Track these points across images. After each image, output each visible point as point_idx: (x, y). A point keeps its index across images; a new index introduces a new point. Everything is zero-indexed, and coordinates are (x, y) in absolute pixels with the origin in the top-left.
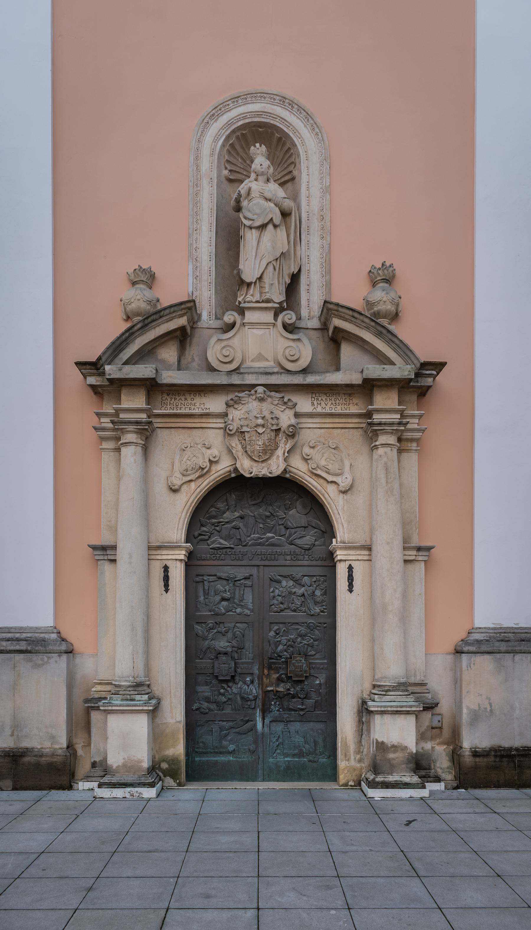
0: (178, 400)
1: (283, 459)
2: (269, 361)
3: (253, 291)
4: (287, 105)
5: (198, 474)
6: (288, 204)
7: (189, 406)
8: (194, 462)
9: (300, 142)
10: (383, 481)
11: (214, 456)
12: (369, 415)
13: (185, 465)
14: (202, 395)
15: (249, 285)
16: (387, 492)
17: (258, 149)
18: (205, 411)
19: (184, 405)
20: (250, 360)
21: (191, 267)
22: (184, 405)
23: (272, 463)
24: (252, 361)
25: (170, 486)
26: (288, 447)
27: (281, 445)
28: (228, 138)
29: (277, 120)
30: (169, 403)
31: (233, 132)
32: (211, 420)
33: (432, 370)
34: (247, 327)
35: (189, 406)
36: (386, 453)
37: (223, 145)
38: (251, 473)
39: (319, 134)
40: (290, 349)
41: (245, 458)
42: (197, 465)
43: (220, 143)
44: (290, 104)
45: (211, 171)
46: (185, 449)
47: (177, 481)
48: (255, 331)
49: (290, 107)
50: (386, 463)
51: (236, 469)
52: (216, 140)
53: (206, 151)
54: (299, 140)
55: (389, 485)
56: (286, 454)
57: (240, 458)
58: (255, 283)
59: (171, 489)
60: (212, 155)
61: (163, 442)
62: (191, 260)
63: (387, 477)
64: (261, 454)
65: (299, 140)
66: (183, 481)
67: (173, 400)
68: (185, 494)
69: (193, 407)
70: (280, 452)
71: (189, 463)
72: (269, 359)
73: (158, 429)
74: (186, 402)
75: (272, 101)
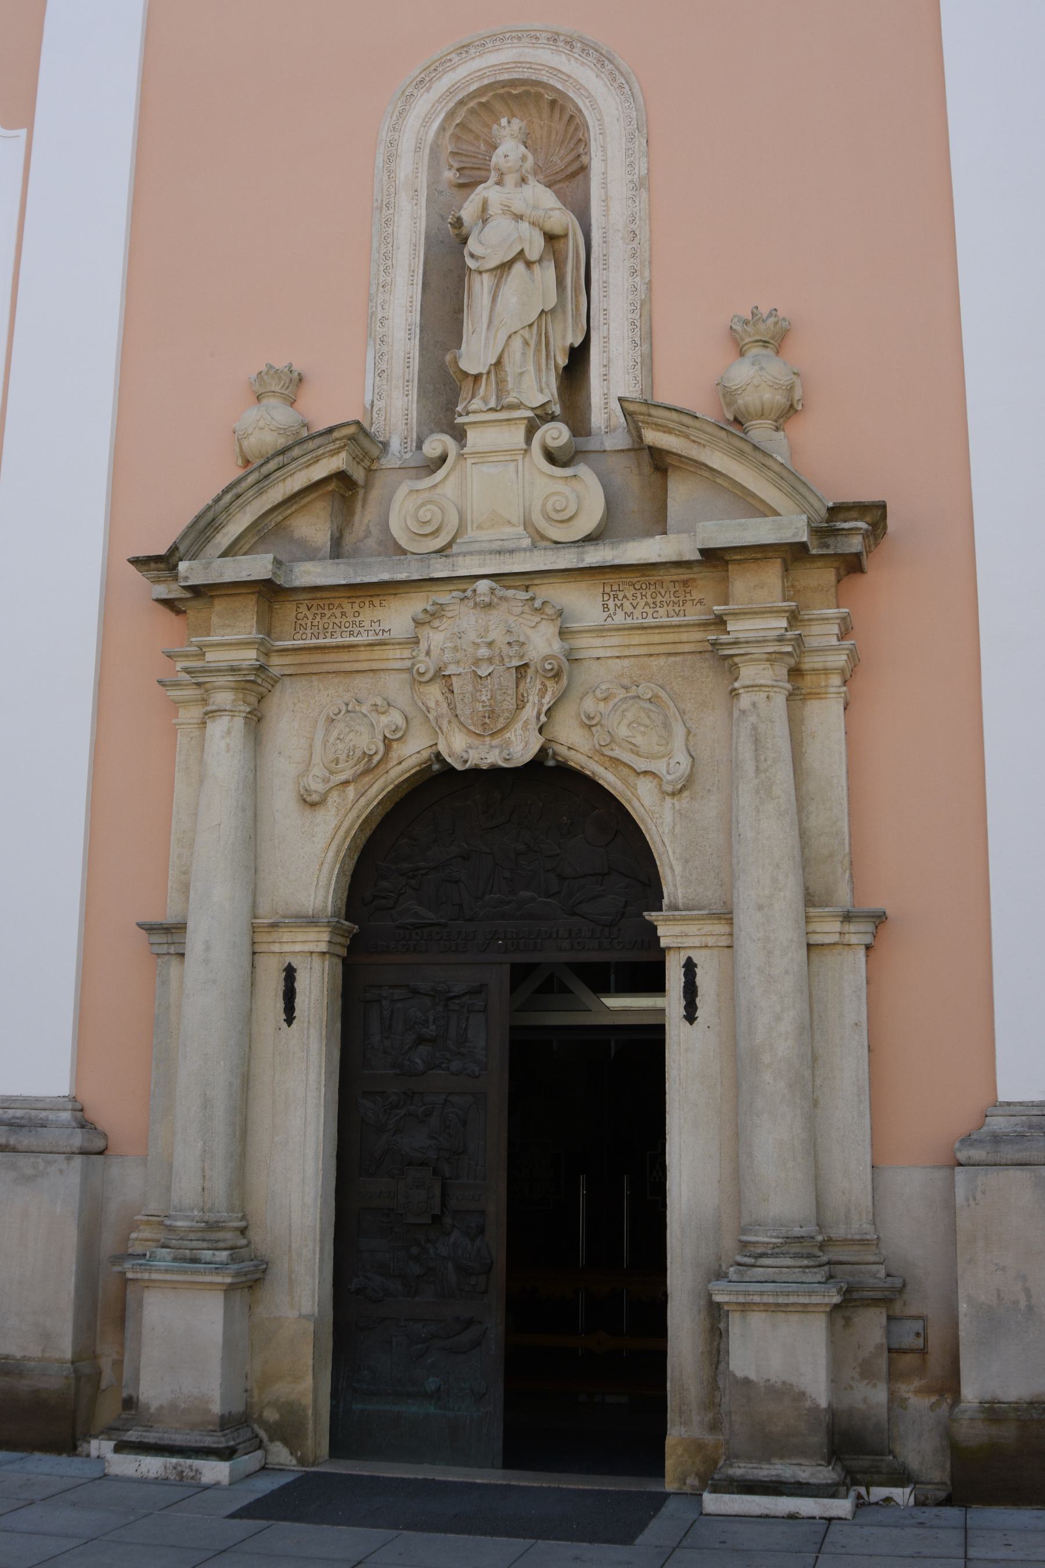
0: (327, 616)
1: (537, 728)
2: (514, 525)
3: (486, 391)
4: (562, 44)
5: (361, 767)
6: (561, 218)
7: (350, 629)
8: (351, 744)
9: (588, 104)
10: (749, 766)
11: (394, 728)
12: (720, 622)
13: (333, 750)
14: (376, 602)
15: (477, 377)
16: (757, 792)
17: (504, 127)
18: (380, 637)
19: (340, 627)
20: (475, 525)
21: (370, 356)
22: (340, 627)
23: (513, 738)
24: (480, 527)
25: (302, 796)
26: (547, 701)
27: (531, 698)
28: (451, 114)
29: (543, 72)
30: (309, 625)
31: (461, 103)
32: (391, 654)
33: (856, 520)
34: (469, 461)
35: (350, 629)
36: (754, 705)
37: (442, 128)
38: (466, 761)
39: (626, 86)
40: (556, 498)
41: (456, 729)
42: (356, 750)
43: (436, 125)
44: (567, 43)
45: (417, 177)
46: (334, 717)
47: (317, 786)
48: (485, 468)
49: (568, 47)
50: (755, 728)
51: (438, 755)
52: (426, 122)
53: (407, 143)
54: (587, 101)
55: (763, 776)
56: (543, 718)
57: (445, 730)
58: (488, 373)
59: (305, 801)
60: (418, 149)
61: (294, 704)
62: (371, 343)
63: (757, 759)
64: (487, 721)
65: (587, 101)
66: (331, 784)
67: (318, 618)
68: (333, 811)
69: (356, 630)
70: (529, 712)
71: (341, 746)
72: (514, 520)
73: (285, 678)
74: (344, 620)
75: (534, 41)
